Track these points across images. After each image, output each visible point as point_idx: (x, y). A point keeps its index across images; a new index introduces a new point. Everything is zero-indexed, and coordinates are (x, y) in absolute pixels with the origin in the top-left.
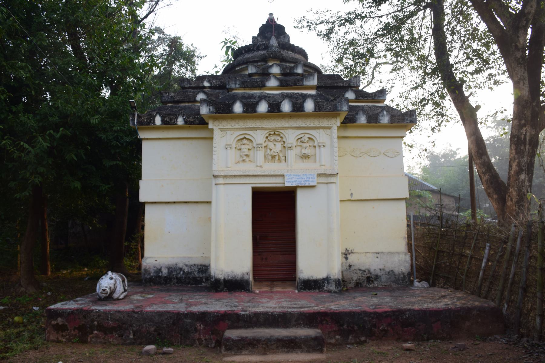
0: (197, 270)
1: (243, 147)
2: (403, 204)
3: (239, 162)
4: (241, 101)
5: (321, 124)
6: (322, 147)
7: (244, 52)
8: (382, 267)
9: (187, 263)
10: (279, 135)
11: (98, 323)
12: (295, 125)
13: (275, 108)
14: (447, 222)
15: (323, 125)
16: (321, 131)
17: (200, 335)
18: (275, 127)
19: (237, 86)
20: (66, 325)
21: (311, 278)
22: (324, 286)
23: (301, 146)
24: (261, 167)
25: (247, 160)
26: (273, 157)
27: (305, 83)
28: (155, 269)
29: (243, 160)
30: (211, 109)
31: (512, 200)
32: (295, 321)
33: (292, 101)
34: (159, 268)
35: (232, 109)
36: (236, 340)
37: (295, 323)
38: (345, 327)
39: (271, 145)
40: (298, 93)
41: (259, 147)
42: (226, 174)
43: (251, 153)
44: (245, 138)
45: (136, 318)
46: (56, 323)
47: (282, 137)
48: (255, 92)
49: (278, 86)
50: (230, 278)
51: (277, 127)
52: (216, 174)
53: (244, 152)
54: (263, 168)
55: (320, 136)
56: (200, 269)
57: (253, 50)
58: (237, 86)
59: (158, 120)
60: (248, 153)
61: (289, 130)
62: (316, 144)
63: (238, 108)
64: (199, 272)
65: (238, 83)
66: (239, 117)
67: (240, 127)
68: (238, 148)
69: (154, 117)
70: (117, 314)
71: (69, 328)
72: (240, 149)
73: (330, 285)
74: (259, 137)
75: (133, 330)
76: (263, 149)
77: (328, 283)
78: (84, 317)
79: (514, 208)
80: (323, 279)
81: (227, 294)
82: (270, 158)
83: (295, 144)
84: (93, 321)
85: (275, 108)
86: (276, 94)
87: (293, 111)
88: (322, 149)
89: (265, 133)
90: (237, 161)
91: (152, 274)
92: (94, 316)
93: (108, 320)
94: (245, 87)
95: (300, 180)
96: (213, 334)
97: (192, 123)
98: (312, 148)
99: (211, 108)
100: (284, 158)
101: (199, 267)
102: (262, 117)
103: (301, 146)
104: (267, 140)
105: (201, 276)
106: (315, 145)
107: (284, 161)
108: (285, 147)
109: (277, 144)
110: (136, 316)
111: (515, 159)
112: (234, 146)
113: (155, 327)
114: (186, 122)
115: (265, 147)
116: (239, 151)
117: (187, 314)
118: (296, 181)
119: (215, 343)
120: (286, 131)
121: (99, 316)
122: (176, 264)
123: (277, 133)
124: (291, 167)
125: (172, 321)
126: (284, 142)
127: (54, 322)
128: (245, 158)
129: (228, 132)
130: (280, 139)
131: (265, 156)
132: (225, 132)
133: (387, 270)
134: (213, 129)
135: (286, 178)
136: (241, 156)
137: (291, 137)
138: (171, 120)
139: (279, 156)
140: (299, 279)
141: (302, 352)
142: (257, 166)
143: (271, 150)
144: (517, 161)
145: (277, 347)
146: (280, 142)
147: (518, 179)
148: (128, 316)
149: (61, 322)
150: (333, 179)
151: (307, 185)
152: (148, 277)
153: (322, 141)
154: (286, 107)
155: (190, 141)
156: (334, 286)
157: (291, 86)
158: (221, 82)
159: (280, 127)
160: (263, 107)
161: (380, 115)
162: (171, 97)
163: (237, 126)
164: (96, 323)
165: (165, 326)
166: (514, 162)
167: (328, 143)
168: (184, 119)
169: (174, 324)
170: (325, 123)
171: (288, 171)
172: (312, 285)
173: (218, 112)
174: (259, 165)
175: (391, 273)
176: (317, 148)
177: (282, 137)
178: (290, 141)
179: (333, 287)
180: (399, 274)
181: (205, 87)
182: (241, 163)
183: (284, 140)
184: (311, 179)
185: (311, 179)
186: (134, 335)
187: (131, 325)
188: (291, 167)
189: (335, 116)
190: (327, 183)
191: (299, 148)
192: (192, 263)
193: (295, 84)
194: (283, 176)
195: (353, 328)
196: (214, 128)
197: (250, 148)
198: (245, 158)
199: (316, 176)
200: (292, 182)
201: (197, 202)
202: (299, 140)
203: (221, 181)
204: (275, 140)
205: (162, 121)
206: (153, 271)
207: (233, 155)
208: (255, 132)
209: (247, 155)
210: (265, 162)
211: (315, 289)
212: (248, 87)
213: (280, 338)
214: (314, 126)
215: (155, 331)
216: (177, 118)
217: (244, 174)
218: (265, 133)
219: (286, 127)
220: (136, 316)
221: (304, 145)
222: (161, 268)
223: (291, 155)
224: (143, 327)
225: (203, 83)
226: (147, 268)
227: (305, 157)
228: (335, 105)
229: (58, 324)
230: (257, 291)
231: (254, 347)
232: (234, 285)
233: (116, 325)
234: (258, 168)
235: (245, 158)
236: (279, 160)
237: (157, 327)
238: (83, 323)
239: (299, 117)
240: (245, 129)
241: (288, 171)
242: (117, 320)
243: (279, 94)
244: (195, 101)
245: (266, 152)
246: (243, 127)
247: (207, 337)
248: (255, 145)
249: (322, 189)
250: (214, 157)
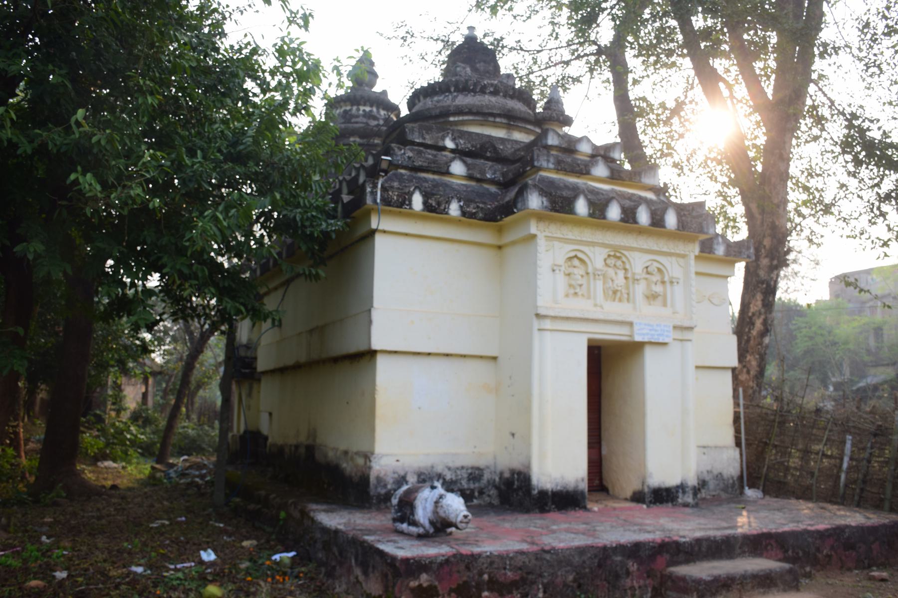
0: (465, 476)
2: (729, 376)
4: (586, 196)
7: (452, 89)
8: (709, 468)
9: (451, 465)
10: (619, 258)
11: (489, 576)
12: (645, 247)
14: (788, 404)
15: (678, 252)
16: (674, 259)
17: (632, 580)
20: (436, 587)
21: (663, 486)
22: (678, 497)
23: (646, 279)
24: (601, 307)
26: (615, 292)
28: (396, 476)
31: (748, 372)
32: (740, 548)
33: (651, 210)
34: (402, 473)
36: (709, 581)
37: (738, 551)
38: (790, 553)
42: (557, 314)
44: (576, 256)
45: (548, 561)
46: (417, 583)
47: (623, 262)
49: (608, 177)
50: (559, 488)
52: (542, 312)
55: (674, 268)
56: (471, 474)
57: (474, 91)
58: (551, 166)
59: (417, 201)
64: (469, 480)
65: (552, 160)
66: (580, 223)
67: (573, 238)
69: (411, 194)
70: (520, 557)
71: (441, 592)
72: (569, 275)
73: (687, 495)
74: (597, 257)
75: (543, 584)
77: (684, 492)
78: (468, 568)
79: (751, 384)
80: (678, 487)
81: (538, 515)
82: (611, 293)
84: (481, 574)
87: (622, 220)
91: (389, 487)
92: (483, 564)
93: (505, 569)
95: (653, 332)
96: (648, 577)
97: (472, 216)
99: (544, 199)
100: (626, 296)
101: (470, 471)
102: (611, 227)
105: (472, 486)
110: (548, 557)
111: (760, 314)
113: (574, 574)
114: (464, 214)
117: (616, 547)
118: (647, 334)
119: (652, 591)
120: (631, 253)
121: (492, 563)
122: (432, 467)
123: (618, 254)
125: (596, 561)
127: (413, 584)
128: (573, 291)
129: (556, 243)
133: (715, 472)
135: (636, 327)
136: (570, 286)
137: (638, 262)
138: (439, 204)
139: (621, 293)
140: (648, 487)
141: (778, 591)
142: (596, 305)
144: (763, 317)
145: (753, 587)
147: (760, 344)
148: (537, 559)
149: (427, 581)
150: (687, 335)
151: (661, 341)
152: (383, 491)
154: (614, 213)
155: (456, 247)
156: (691, 496)
158: (472, 146)
161: (715, 241)
162: (409, 158)
164: (486, 577)
165: (587, 570)
166: (759, 317)
168: (461, 207)
169: (600, 566)
172: (663, 496)
173: (554, 209)
175: (719, 477)
176: (668, 285)
177: (623, 262)
179: (689, 499)
180: (728, 479)
181: (444, 148)
183: (628, 267)
184: (666, 333)
185: (666, 333)
186: (545, 592)
187: (541, 576)
190: (681, 340)
192: (459, 463)
193: (630, 180)
194: (631, 324)
195: (797, 553)
196: (538, 233)
198: (573, 291)
199: (671, 328)
200: (644, 334)
201: (464, 356)
203: (547, 324)
205: (425, 203)
206: (391, 481)
208: (592, 248)
211: (667, 502)
213: (755, 573)
214: (658, 249)
215: (575, 580)
216: (448, 202)
217: (582, 316)
220: (548, 557)
222: (406, 474)
224: (557, 577)
225: (443, 139)
226: (382, 475)
228: (701, 224)
229: (420, 585)
230: (596, 509)
231: (728, 591)
232: (565, 500)
233: (517, 578)
237: (577, 574)
238: (465, 579)
239: (630, 231)
242: (520, 569)
244: (448, 173)
246: (579, 238)
247: (642, 582)
249: (675, 349)
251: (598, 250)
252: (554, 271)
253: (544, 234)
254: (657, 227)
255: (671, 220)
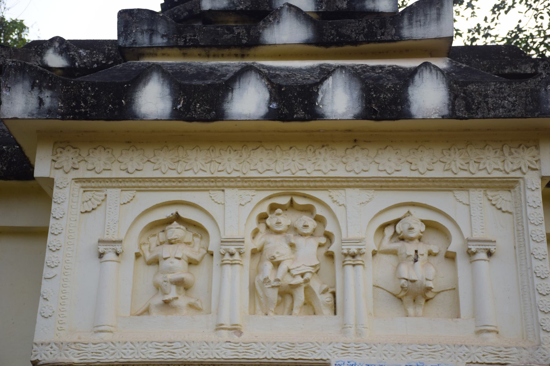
1: (167, 251)
3: (147, 311)
5: (473, 168)
6: (483, 255)
10: (308, 210)
12: (373, 172)
13: (294, 102)
16: (476, 196)
18: (296, 179)
19: (159, 40)
23: (394, 253)
25: (182, 301)
26: (286, 293)
27: (406, 33)
29: (166, 303)
30: (48, 102)
35: (131, 102)
39: (278, 246)
40: (381, 67)
41: (230, 254)
43: (198, 277)
44: (177, 218)
47: (319, 220)
48: (224, 62)
49: (307, 43)
51: (301, 180)
53: (171, 270)
54: (245, 337)
55: (473, 216)
60: (187, 277)
61: (349, 191)
62: (455, 245)
63: (153, 99)
66: (153, 138)
67: (157, 174)
68: (149, 256)
72: (155, 262)
74: (233, 214)
76: (247, 261)
82: (273, 295)
83: (371, 245)
85: (294, 102)
86: (300, 70)
88: (483, 265)
89: (256, 200)
90: (141, 307)
94: (185, 46)
98: (440, 262)
99: (47, 96)
100: (327, 297)
102: (247, 138)
103: (394, 253)
104: (262, 228)
106: (451, 248)
107: (327, 312)
108: (330, 256)
109: (300, 241)
112: (131, 246)
115: (255, 253)
116: (152, 269)
120: (339, 195)
123: (299, 201)
124: (359, 333)
126: (329, 236)
129: (114, 194)
130: (312, 224)
131: (253, 290)
132: (99, 196)
134: (50, 181)
136: (158, 287)
137: (356, 216)
139: (308, 289)
142: (219, 327)
143: (277, 264)
146: (312, 235)
153: (477, 235)
157: (355, 43)
159: (314, 180)
160: (249, 101)
163: (148, 171)
167: (504, 244)
170: (490, 164)
171: (345, 349)
173: (72, 112)
174: (228, 325)
176: (461, 262)
177: (319, 220)
178: (353, 234)
182: (154, 313)
183: (330, 227)
188: (359, 333)
189: (532, 139)
191: (387, 261)
193: (371, 38)
196: (58, 176)
197: (196, 256)
202: (389, 231)
204: (293, 228)
207: (123, 281)
208: (218, 195)
209: (180, 283)
210: (253, 312)
212: (196, 45)
218: (256, 200)
219: (335, 179)
221: (409, 249)
223: (359, 285)
227: (414, 295)
234: (225, 335)
235: (172, 293)
236: (309, 305)
240: (181, 184)
241: (345, 349)
243: (311, 70)
245: (258, 271)
248: (214, 244)
250: (46, 286)
251: (232, 196)
252: (101, 255)
253: (74, 174)
254: (397, 119)
255: (429, 96)
